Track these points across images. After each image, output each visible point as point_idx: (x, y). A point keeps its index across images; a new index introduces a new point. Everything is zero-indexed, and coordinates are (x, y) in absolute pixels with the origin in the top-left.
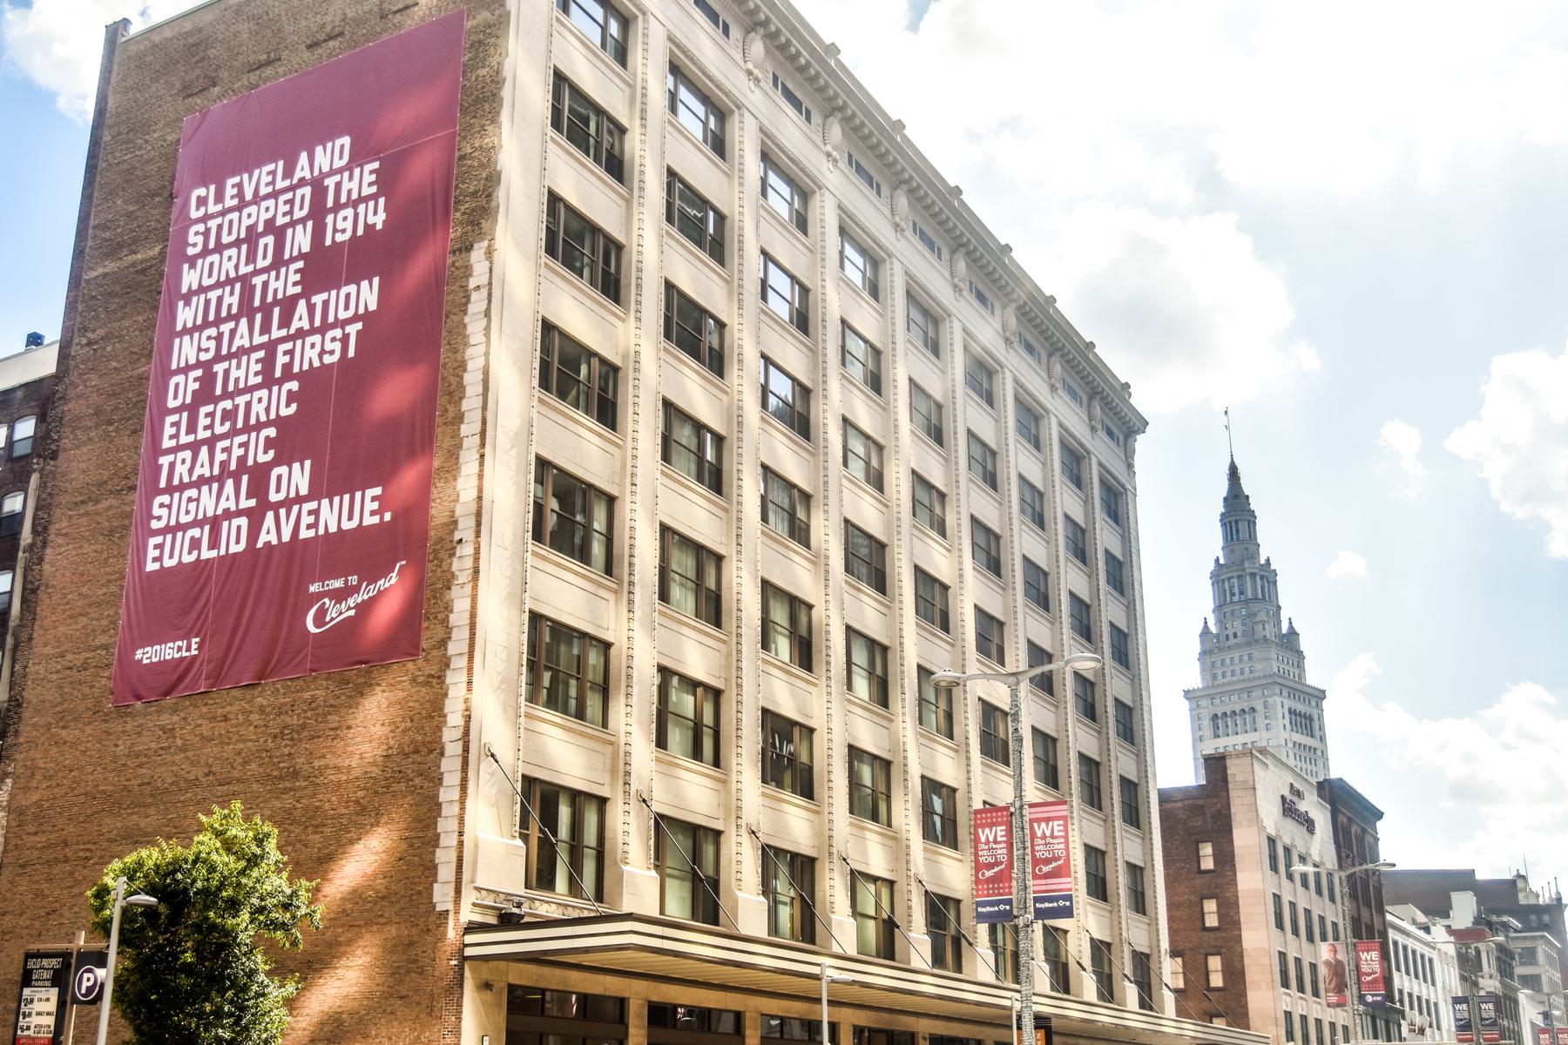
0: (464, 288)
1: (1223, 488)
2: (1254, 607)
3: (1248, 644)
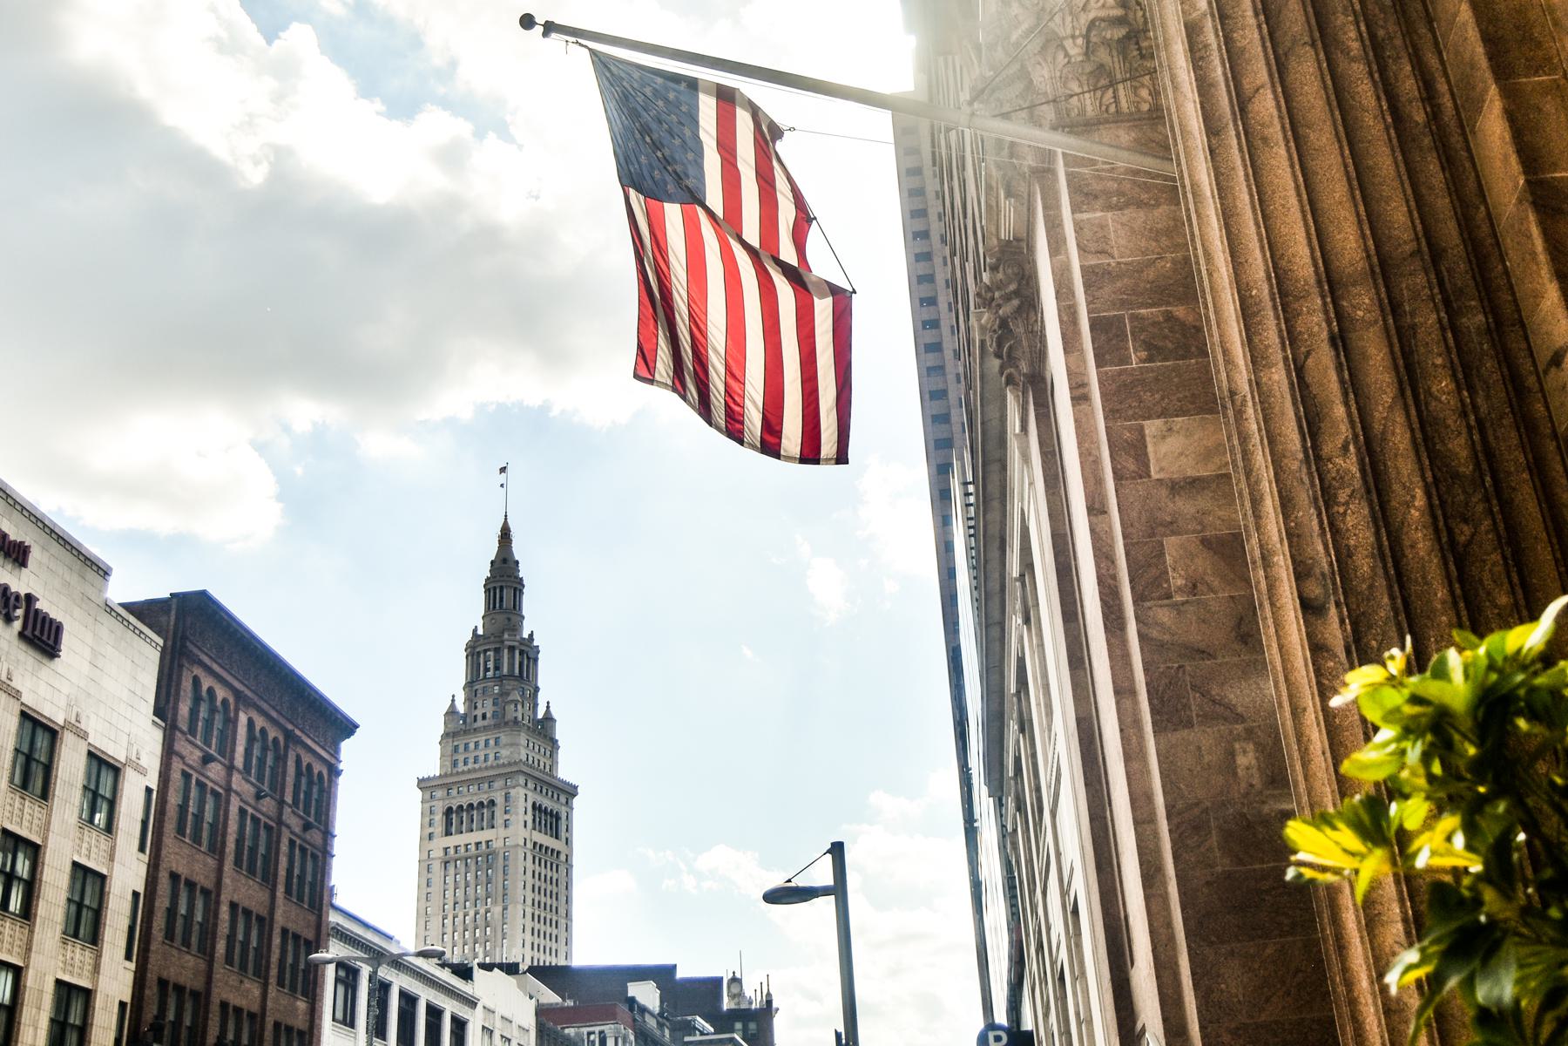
2: (509, 685)
3: (497, 726)
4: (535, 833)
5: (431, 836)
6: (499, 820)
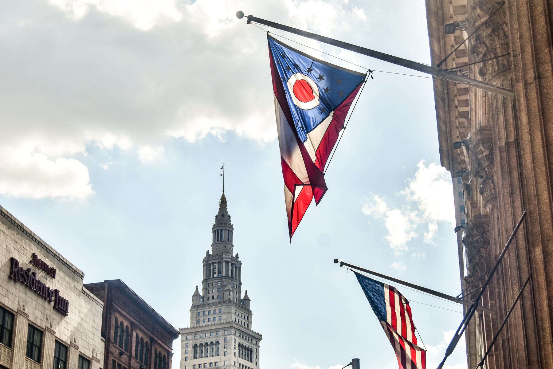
2: (225, 281)
3: (220, 303)
4: (240, 359)
5: (186, 359)
6: (221, 352)
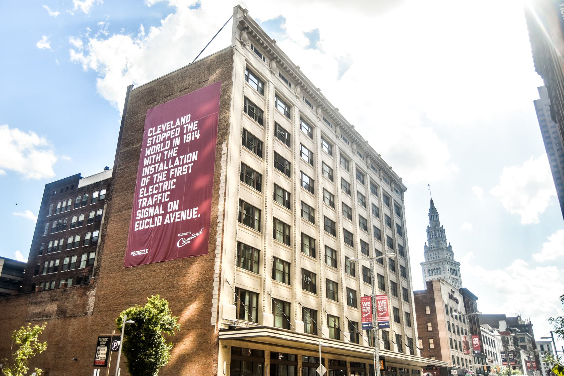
0: (220, 154)
1: (429, 206)
2: (439, 239)
3: (438, 250)
